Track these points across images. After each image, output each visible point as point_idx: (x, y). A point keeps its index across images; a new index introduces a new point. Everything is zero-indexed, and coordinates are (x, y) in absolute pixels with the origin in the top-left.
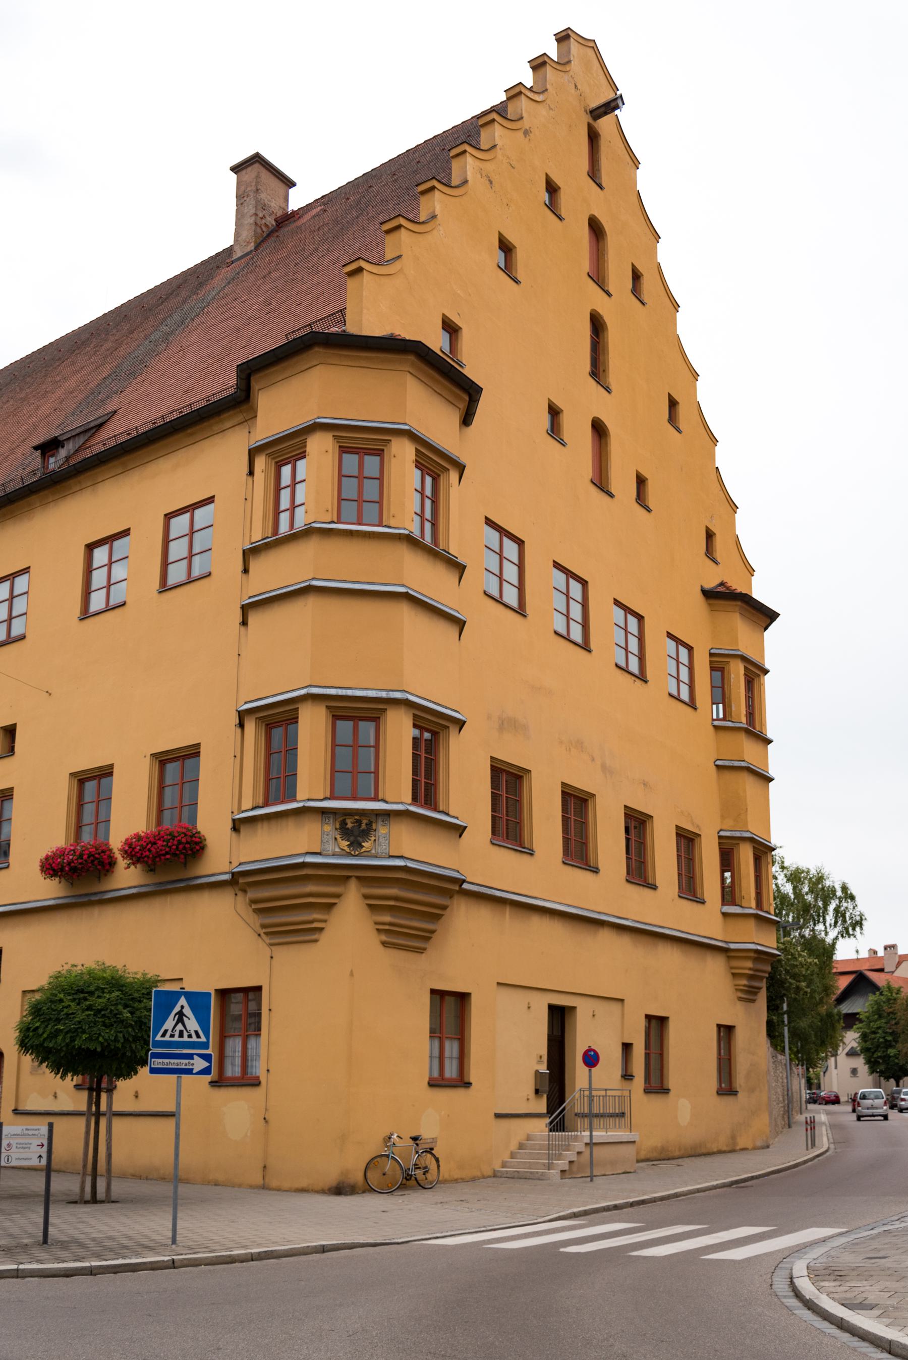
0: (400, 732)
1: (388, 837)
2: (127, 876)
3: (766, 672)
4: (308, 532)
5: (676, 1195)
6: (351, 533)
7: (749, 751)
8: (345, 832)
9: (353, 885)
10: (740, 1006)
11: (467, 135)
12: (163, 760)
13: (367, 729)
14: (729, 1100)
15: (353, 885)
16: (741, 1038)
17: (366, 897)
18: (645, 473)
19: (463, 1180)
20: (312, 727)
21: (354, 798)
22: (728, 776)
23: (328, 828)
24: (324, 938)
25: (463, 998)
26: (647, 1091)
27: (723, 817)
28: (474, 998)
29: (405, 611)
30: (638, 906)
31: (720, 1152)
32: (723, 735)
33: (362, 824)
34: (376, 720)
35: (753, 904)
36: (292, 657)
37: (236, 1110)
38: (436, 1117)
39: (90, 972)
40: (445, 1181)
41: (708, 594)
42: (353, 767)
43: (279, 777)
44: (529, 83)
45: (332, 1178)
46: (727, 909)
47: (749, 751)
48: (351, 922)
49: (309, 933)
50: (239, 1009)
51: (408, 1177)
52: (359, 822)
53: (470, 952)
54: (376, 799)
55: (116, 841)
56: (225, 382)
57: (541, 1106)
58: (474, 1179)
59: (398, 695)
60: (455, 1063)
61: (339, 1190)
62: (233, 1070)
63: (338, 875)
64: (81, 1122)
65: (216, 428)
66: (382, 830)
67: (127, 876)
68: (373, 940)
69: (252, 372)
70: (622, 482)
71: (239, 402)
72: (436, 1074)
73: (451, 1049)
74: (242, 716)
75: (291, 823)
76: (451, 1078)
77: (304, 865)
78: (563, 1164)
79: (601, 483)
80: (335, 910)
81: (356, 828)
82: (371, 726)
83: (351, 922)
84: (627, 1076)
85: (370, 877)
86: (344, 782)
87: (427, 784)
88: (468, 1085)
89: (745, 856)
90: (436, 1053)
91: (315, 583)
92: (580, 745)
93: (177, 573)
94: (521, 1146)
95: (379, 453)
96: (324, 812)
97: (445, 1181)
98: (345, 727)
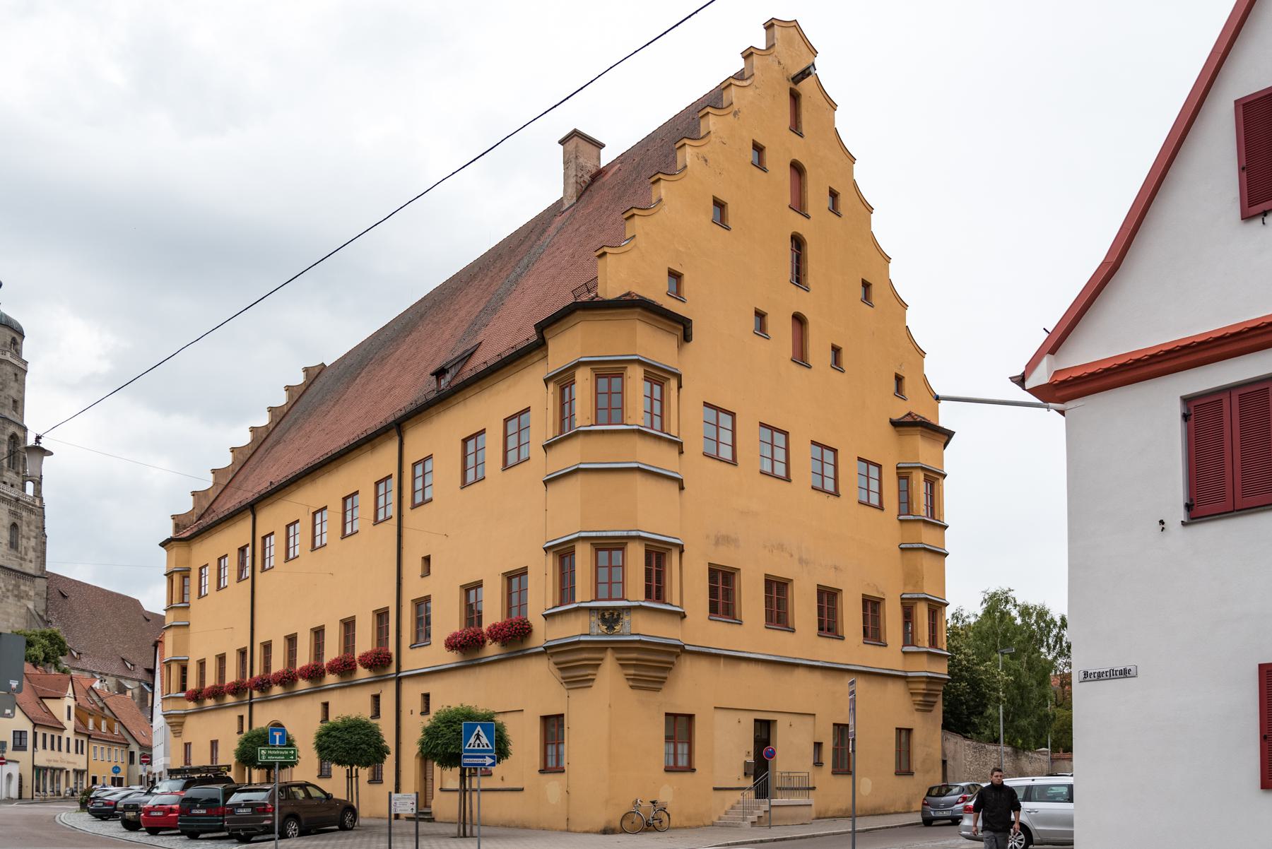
0: (636, 557)
1: (629, 623)
2: (492, 649)
3: (944, 476)
4: (577, 433)
5: (814, 836)
6: (603, 432)
7: (927, 537)
8: (604, 620)
9: (609, 653)
10: (918, 716)
11: (714, 101)
12: (509, 577)
13: (617, 555)
14: (906, 779)
15: (609, 653)
16: (917, 737)
17: (618, 659)
18: (838, 344)
19: (690, 827)
20: (583, 555)
21: (610, 599)
22: (909, 555)
23: (593, 619)
24: (595, 684)
25: (690, 717)
26: (834, 773)
27: (905, 585)
28: (696, 718)
29: (638, 479)
30: (828, 652)
31: (896, 813)
32: (906, 526)
33: (620, 615)
34: (622, 549)
35: (927, 644)
36: (572, 512)
37: (553, 784)
38: (669, 790)
39: (457, 709)
40: (677, 828)
41: (895, 424)
42: (608, 581)
43: (566, 588)
44: (762, 45)
45: (601, 826)
46: (907, 649)
47: (927, 537)
48: (610, 674)
49: (586, 682)
50: (553, 726)
51: (649, 825)
52: (612, 614)
53: (692, 688)
54: (623, 599)
55: (485, 628)
56: (531, 334)
57: (750, 782)
58: (698, 827)
59: (634, 533)
60: (685, 757)
61: (606, 831)
62: (552, 763)
63: (601, 647)
64: (457, 794)
65: (530, 362)
66: (625, 618)
67: (492, 649)
68: (624, 685)
69: (544, 327)
70: (819, 352)
71: (537, 347)
72: (672, 764)
73: (682, 748)
74: (546, 549)
75: (573, 617)
76: (681, 766)
77: (579, 642)
78: (754, 818)
79: (801, 358)
80: (601, 669)
81: (611, 618)
82: (620, 553)
83: (610, 674)
84: (818, 764)
85: (620, 647)
86: (603, 589)
87: (655, 587)
88: (694, 770)
89: (922, 612)
90: (672, 751)
91: (582, 466)
92: (781, 547)
93: (512, 457)
94: (733, 808)
95: (621, 376)
96: (591, 609)
97: (677, 828)
98: (603, 555)
